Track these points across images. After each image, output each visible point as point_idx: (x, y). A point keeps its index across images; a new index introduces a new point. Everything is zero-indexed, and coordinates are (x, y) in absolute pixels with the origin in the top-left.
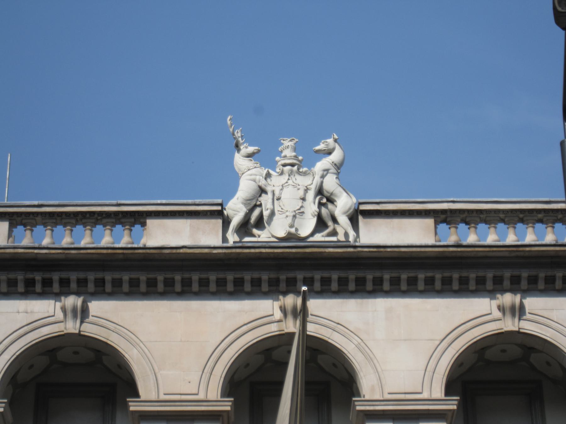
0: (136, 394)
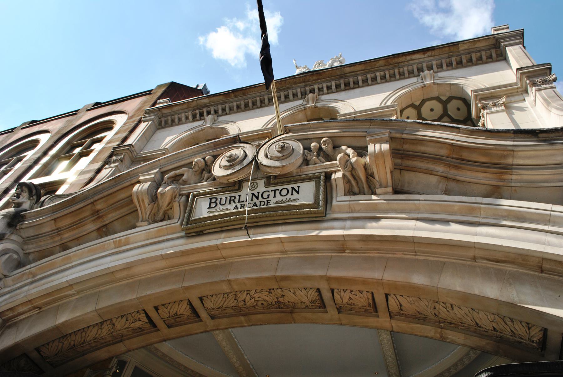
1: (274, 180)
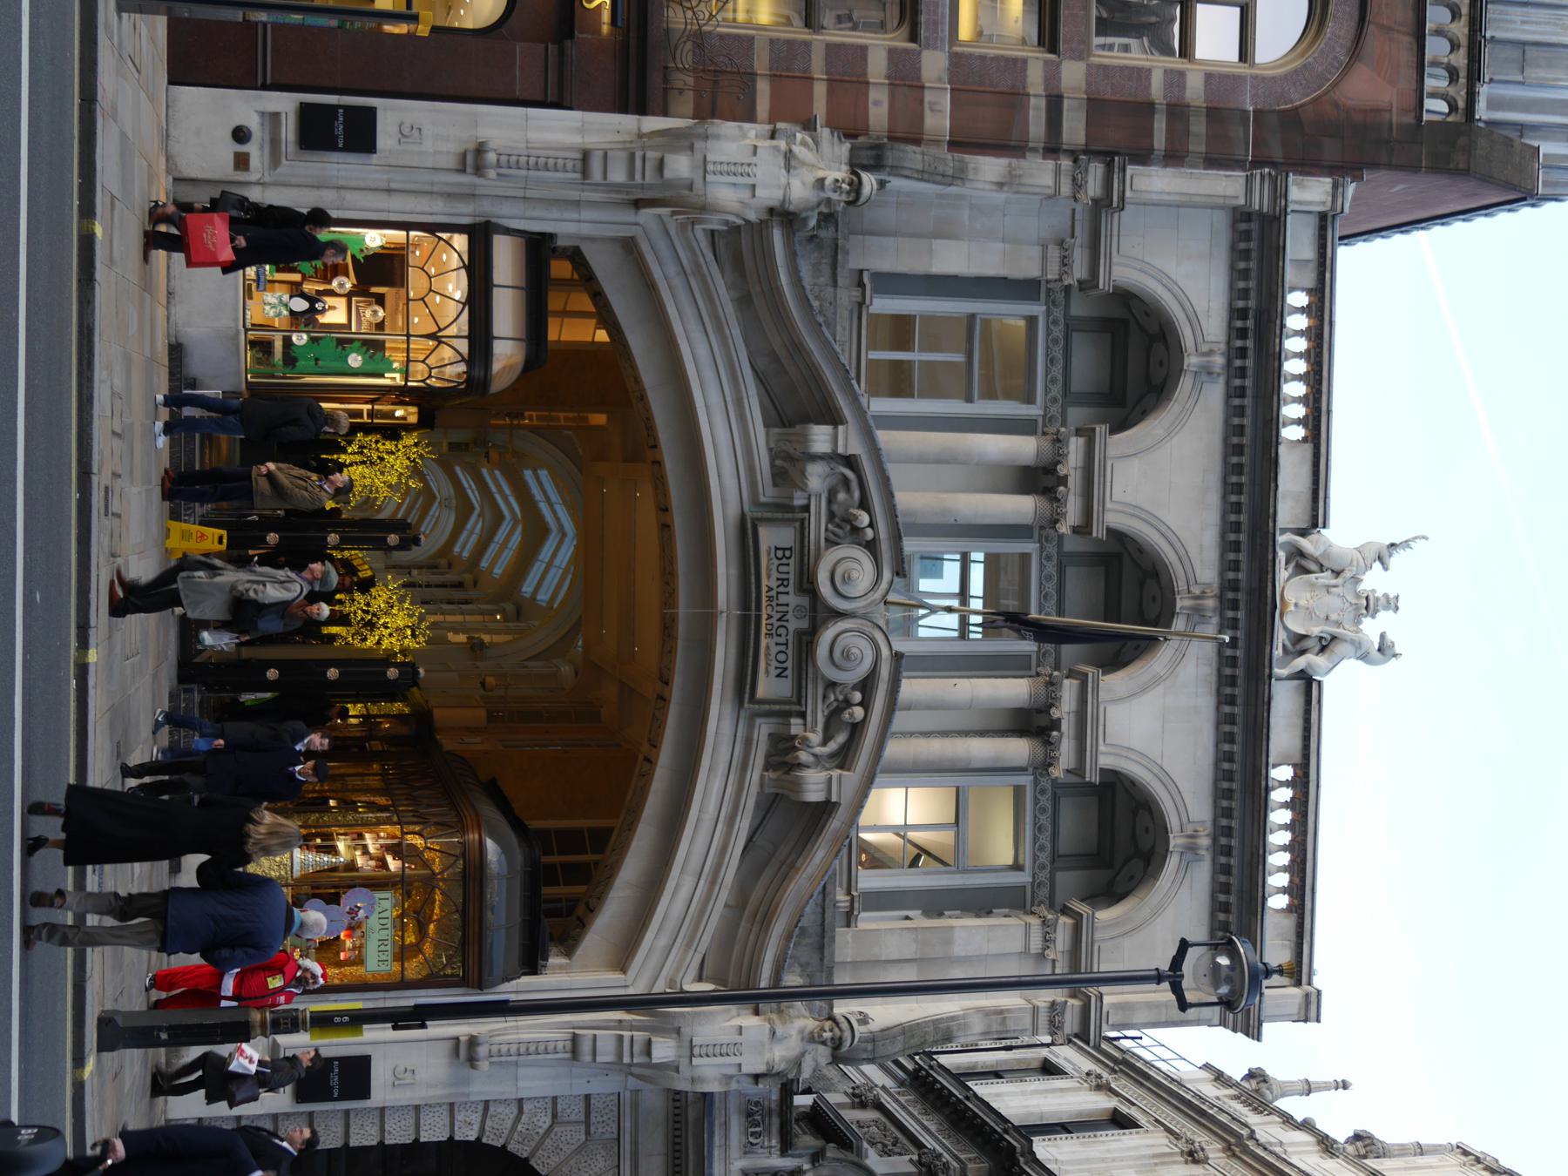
0: (1113, 431)
1: (806, 642)
